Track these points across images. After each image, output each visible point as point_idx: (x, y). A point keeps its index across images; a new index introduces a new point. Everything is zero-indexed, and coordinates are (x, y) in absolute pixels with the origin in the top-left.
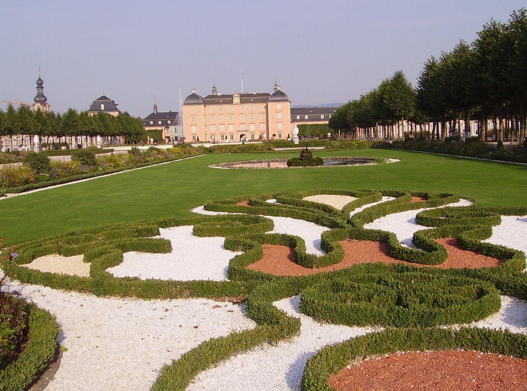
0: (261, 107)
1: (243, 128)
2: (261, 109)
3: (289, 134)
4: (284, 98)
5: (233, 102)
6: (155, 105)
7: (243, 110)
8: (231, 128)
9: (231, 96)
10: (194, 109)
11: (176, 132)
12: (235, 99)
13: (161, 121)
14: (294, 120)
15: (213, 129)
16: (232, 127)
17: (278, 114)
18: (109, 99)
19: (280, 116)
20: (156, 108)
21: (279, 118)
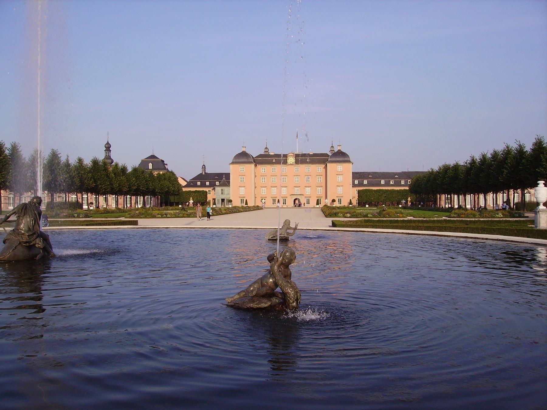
1: (297, 191)
2: (318, 171)
4: (346, 159)
5: (287, 163)
6: (204, 165)
8: (284, 191)
9: (286, 156)
10: (243, 169)
11: (222, 194)
13: (209, 182)
14: (354, 185)
16: (285, 190)
18: (159, 159)
19: (340, 178)
20: (205, 168)
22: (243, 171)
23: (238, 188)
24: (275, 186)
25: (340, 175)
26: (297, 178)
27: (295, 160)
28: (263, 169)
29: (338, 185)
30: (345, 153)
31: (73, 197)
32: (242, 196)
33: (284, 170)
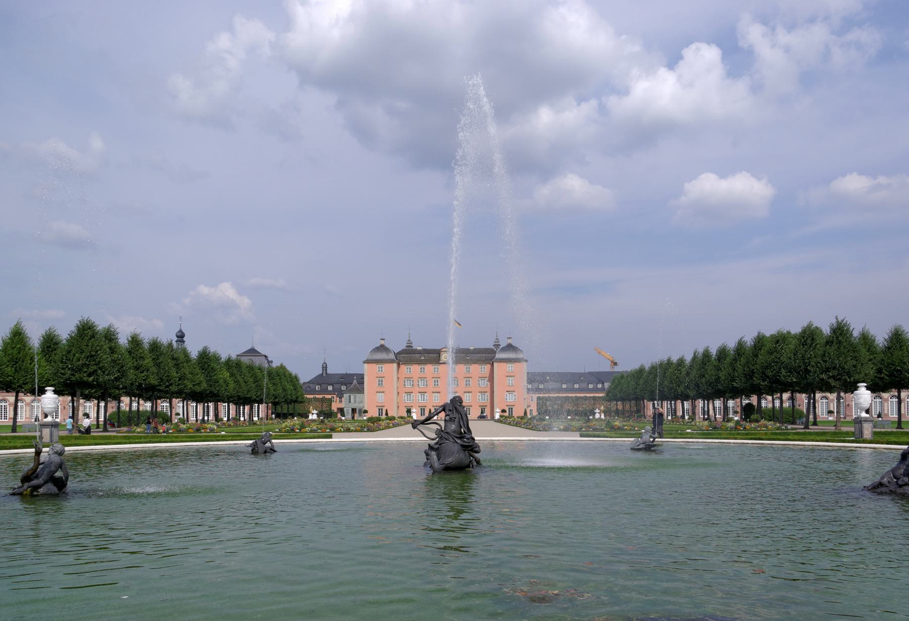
0: (481, 368)
2: (482, 371)
5: (440, 360)
6: (325, 363)
12: (444, 355)
15: (406, 400)
16: (438, 397)
17: (508, 378)
19: (511, 381)
21: (510, 384)
22: (382, 371)
24: (424, 391)
25: (510, 376)
28: (407, 368)
31: (164, 406)
32: (379, 405)
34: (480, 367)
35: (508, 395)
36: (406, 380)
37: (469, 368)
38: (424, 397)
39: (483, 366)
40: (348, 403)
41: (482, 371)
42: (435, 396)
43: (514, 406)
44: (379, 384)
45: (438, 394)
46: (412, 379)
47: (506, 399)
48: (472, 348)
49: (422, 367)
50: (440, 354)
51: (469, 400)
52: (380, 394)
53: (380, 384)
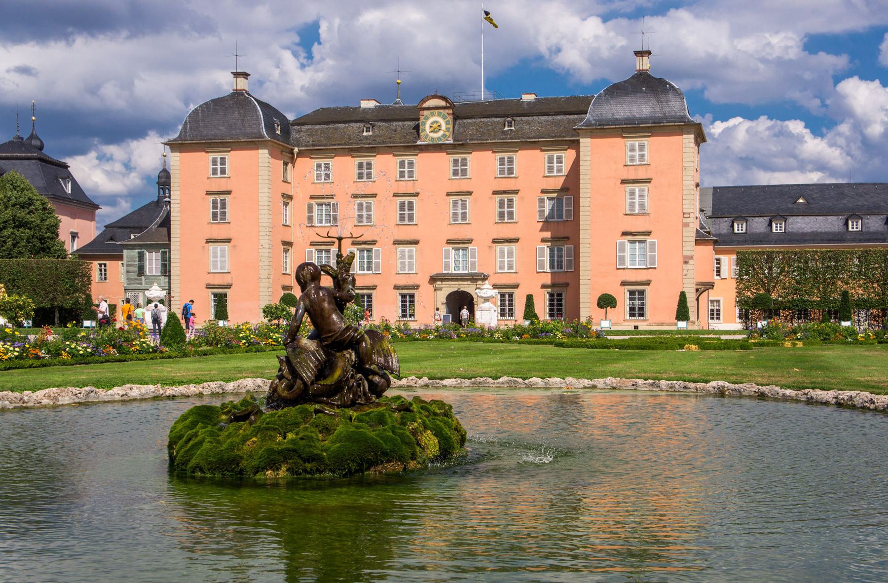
3: (683, 295)
7: (464, 172)
16: (411, 257)
17: (629, 187)
23: (203, 247)
26: (460, 202)
27: (451, 126)
29: (633, 230)
30: (667, 83)
33: (406, 170)
34: (546, 155)
35: (628, 246)
36: (313, 202)
37: (511, 161)
38: (369, 257)
39: (555, 154)
40: (135, 275)
41: (550, 169)
42: (403, 252)
43: (648, 283)
44: (215, 216)
45: (413, 248)
46: (332, 201)
47: (622, 259)
48: (528, 98)
49: (364, 160)
50: (418, 119)
51: (510, 267)
52: (219, 247)
53: (219, 214)
